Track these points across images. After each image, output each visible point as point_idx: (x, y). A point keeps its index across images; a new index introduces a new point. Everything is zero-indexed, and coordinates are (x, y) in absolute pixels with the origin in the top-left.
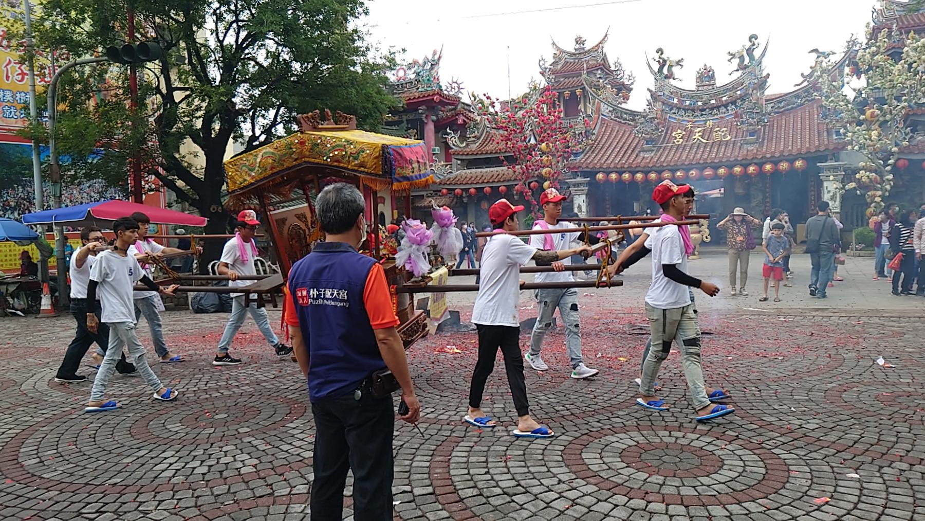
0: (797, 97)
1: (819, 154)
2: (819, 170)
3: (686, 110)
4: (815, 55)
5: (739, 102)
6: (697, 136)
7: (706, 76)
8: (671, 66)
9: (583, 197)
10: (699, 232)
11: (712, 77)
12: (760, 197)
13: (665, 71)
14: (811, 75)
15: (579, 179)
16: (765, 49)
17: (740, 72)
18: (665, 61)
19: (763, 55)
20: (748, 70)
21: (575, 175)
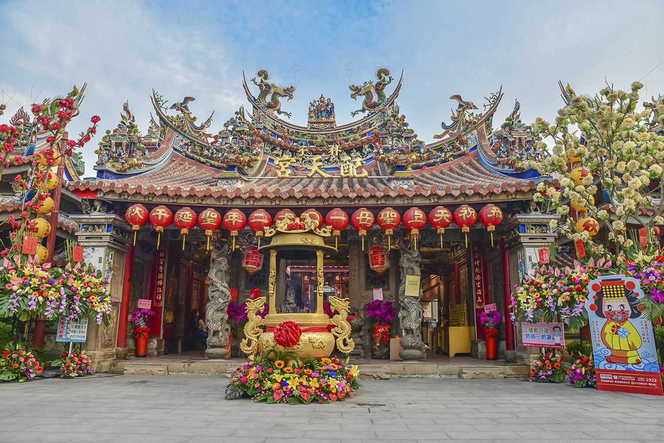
0: (440, 150)
1: (519, 197)
4: (456, 103)
7: (323, 111)
9: (101, 252)
10: (329, 328)
11: (330, 113)
14: (452, 127)
15: (97, 215)
16: (399, 86)
17: (367, 112)
19: (396, 94)
20: (377, 109)
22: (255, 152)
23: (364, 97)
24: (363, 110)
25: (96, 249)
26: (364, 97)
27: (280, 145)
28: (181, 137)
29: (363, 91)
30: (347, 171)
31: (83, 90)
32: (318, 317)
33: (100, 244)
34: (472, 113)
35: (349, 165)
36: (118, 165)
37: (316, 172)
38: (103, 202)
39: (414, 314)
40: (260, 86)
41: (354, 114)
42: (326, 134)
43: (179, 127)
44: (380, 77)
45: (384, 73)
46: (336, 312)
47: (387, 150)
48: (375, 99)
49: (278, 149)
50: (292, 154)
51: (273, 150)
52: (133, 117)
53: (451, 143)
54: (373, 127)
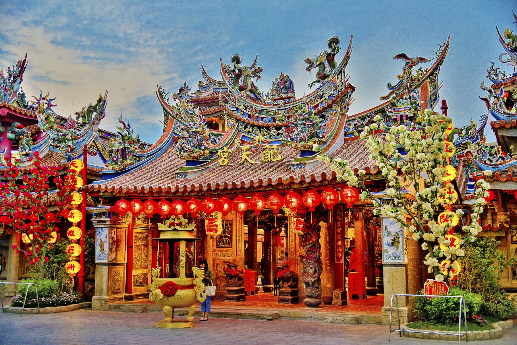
3: (260, 128)
6: (244, 156)
9: (106, 231)
10: (191, 287)
18: (240, 71)
21: (97, 201)
22: (203, 148)
23: (318, 69)
24: (318, 81)
25: (104, 229)
26: (318, 69)
29: (316, 63)
30: (266, 157)
31: (106, 97)
33: (105, 226)
34: (421, 68)
35: (267, 153)
36: (117, 167)
37: (246, 160)
38: (105, 198)
39: (312, 271)
41: (311, 86)
42: (285, 109)
43: (177, 114)
44: (331, 47)
45: (334, 42)
49: (249, 126)
50: (260, 130)
51: (245, 128)
52: (129, 125)
54: (324, 98)
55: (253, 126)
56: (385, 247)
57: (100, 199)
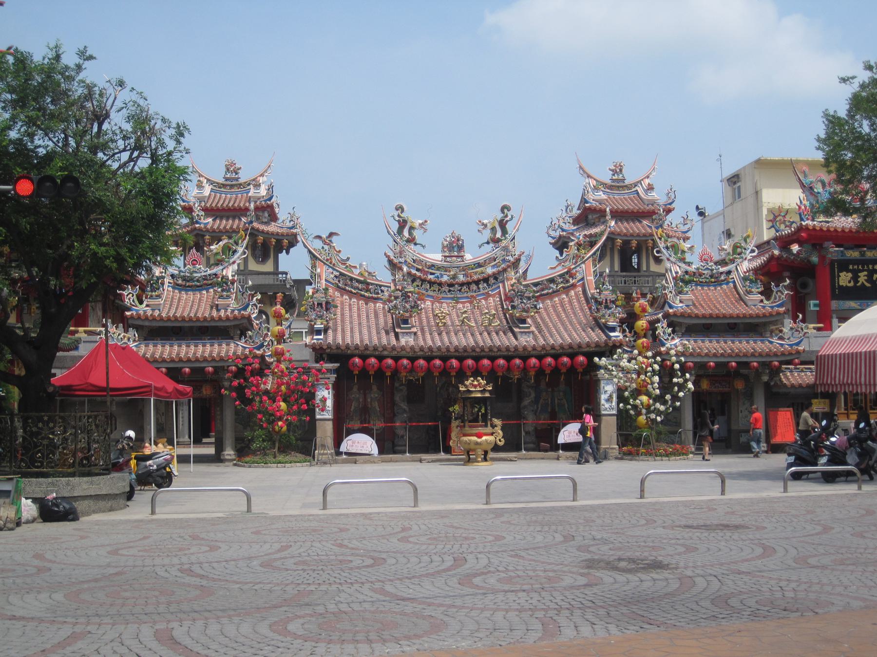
2: (598, 367)
5: (492, 281)
7: (455, 246)
8: (412, 228)
10: (492, 434)
11: (461, 248)
12: (533, 395)
13: (406, 233)
24: (488, 243)
27: (420, 278)
28: (331, 270)
32: (489, 429)
40: (399, 221)
43: (327, 260)
44: (503, 212)
46: (496, 426)
47: (513, 307)
48: (499, 235)
53: (561, 276)
55: (423, 281)
56: (603, 402)
57: (324, 356)
